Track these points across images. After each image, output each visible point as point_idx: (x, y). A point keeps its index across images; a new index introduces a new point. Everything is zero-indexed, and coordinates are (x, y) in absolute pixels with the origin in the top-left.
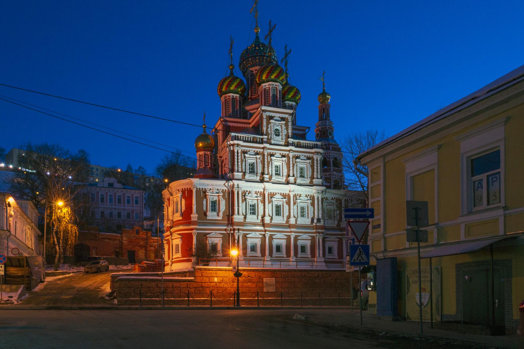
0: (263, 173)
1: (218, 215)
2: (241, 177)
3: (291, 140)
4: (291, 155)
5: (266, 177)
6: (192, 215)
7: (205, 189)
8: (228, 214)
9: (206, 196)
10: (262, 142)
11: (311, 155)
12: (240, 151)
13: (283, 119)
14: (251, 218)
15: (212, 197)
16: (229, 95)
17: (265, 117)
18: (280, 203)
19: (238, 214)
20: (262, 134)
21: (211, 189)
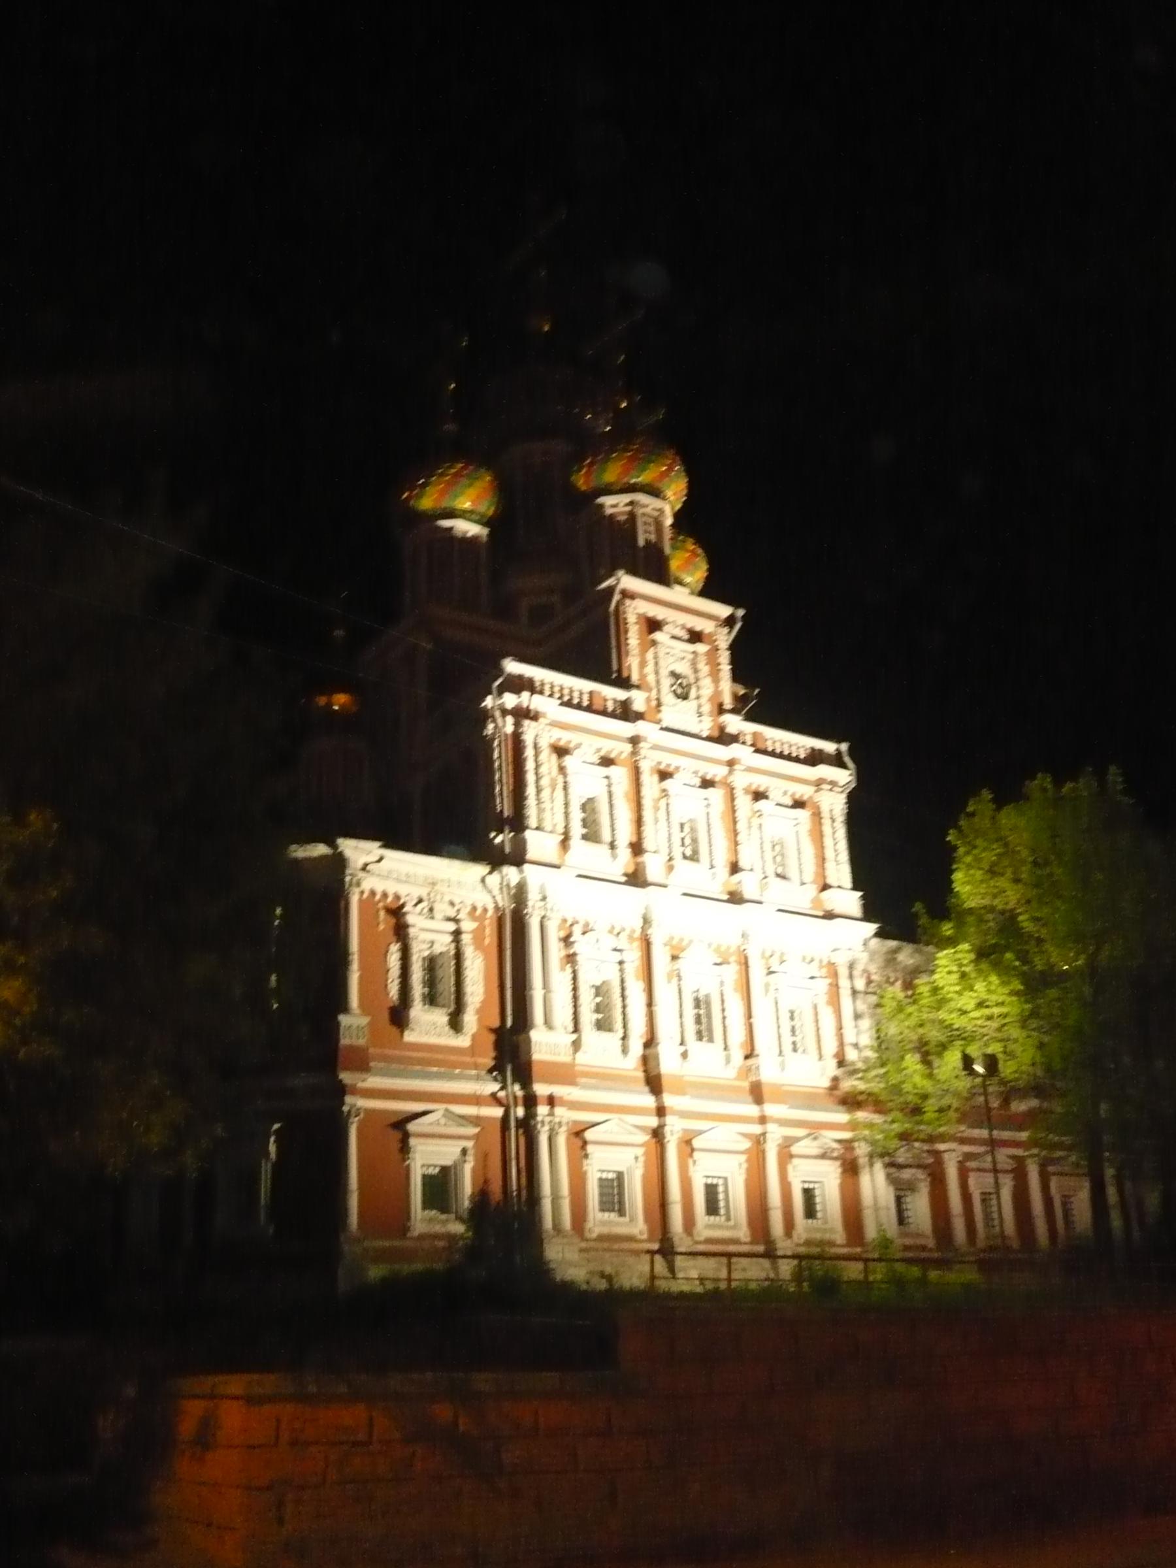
0: (637, 848)
1: (455, 1024)
2: (552, 855)
3: (735, 723)
4: (741, 780)
5: (653, 866)
6: (343, 1019)
7: (397, 897)
8: (496, 1023)
9: (401, 931)
10: (625, 713)
11: (805, 792)
12: (544, 744)
13: (695, 637)
14: (602, 1051)
15: (429, 935)
16: (446, 523)
17: (631, 618)
18: (709, 988)
19: (548, 1023)
20: (623, 682)
21: (420, 901)
